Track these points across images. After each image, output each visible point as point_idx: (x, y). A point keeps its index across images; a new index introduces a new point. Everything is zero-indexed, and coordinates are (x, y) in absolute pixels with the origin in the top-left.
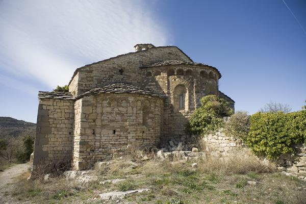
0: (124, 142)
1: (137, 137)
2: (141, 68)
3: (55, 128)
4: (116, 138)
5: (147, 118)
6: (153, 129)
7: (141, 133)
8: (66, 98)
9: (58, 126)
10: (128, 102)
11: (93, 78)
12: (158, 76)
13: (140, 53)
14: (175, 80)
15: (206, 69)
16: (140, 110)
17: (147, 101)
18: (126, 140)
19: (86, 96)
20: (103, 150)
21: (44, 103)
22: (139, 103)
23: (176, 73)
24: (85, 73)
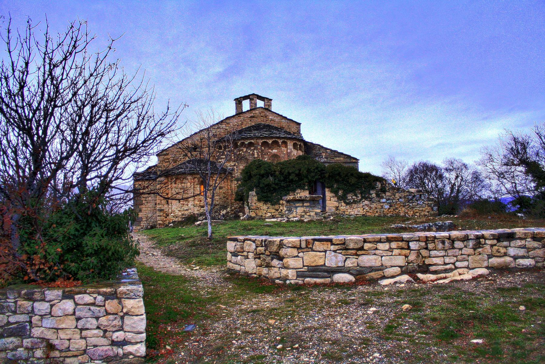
11: (168, 159)
16: (197, 184)
22: (196, 180)
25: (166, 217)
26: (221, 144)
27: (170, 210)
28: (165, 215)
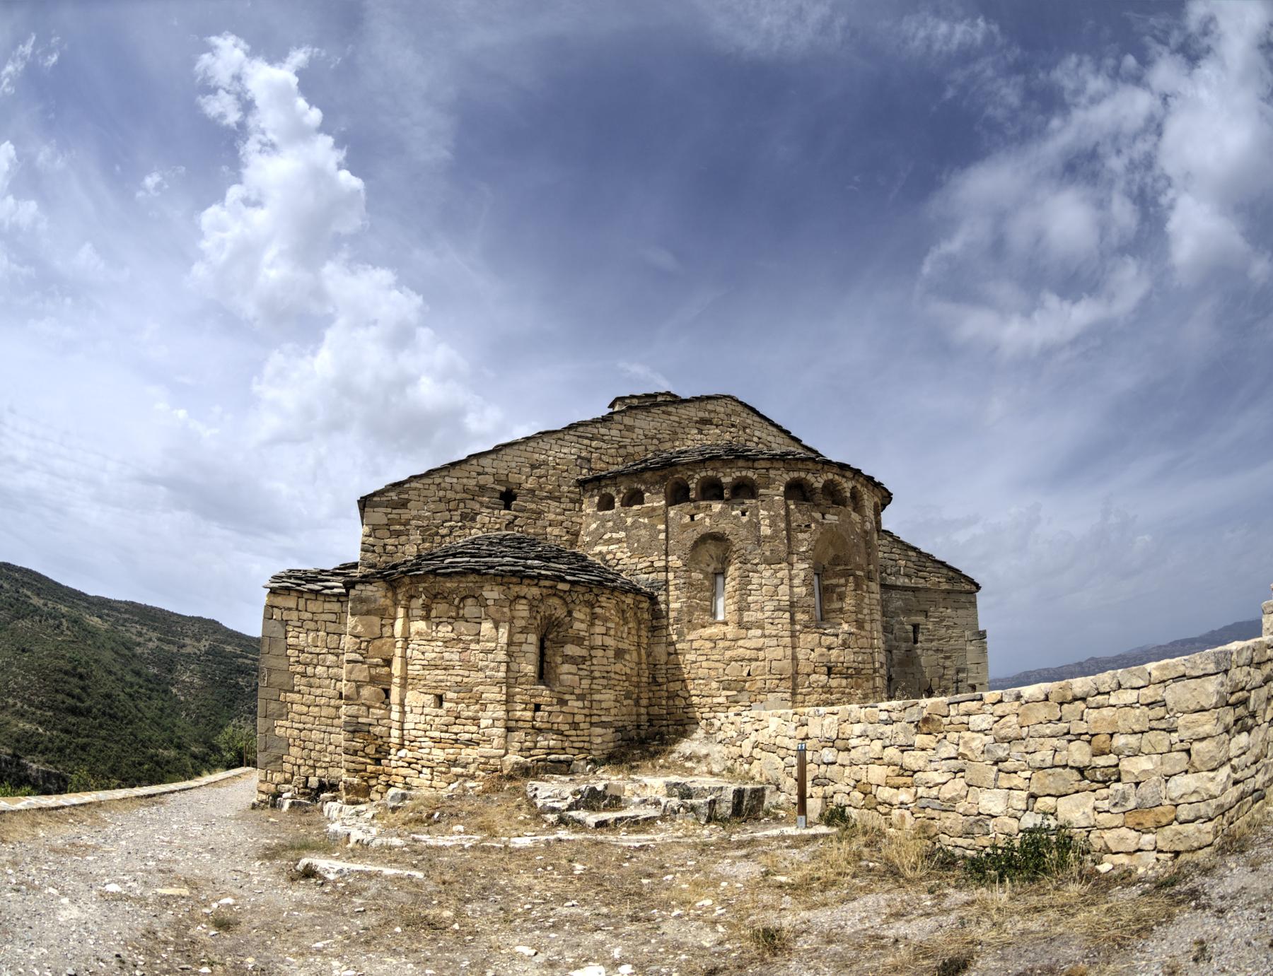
0: (467, 736)
1: (513, 724)
2: (582, 483)
3: (304, 675)
4: (445, 720)
5: (559, 660)
6: (581, 697)
7: (525, 709)
8: (332, 588)
9: (310, 670)
10: (481, 602)
11: (407, 523)
12: (636, 507)
13: (581, 429)
14: (692, 518)
15: (808, 471)
16: (524, 630)
17: (555, 601)
18: (475, 729)
19: (363, 583)
20: (410, 754)
21: (279, 601)
22: (522, 609)
23: (692, 495)
24: (384, 510)
25: (378, 762)
26: (611, 490)
27: (395, 733)
28: (371, 750)
